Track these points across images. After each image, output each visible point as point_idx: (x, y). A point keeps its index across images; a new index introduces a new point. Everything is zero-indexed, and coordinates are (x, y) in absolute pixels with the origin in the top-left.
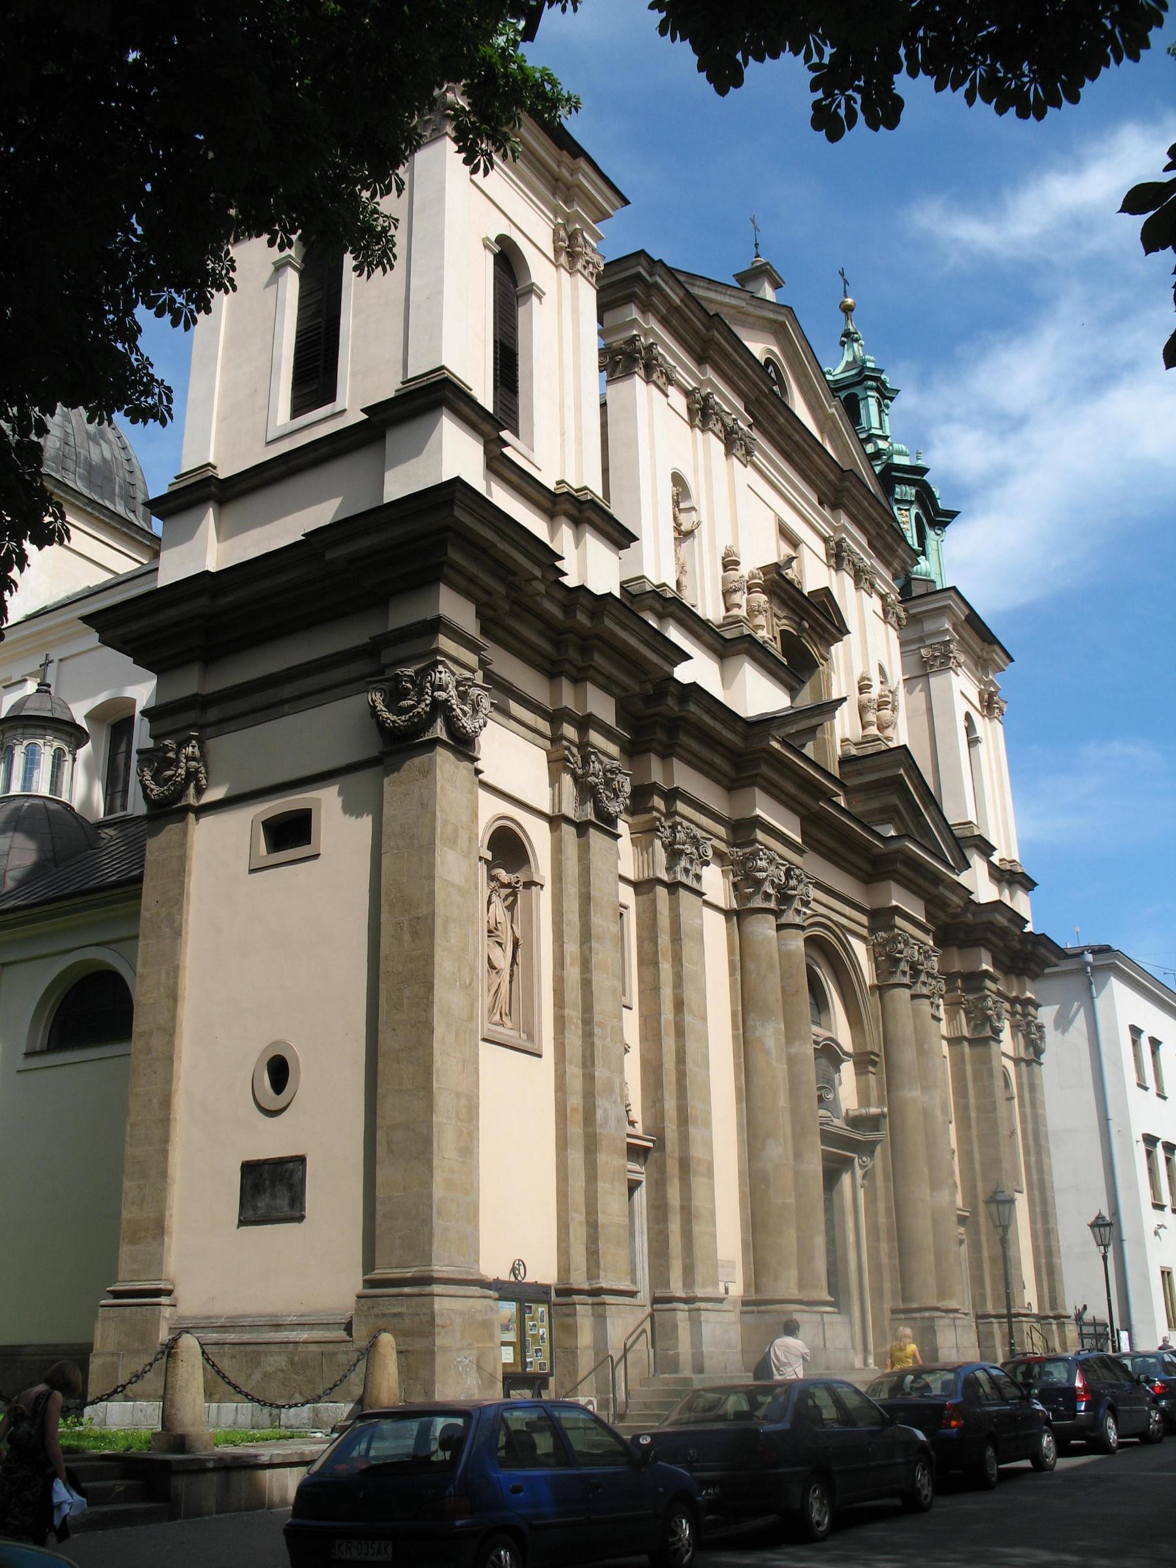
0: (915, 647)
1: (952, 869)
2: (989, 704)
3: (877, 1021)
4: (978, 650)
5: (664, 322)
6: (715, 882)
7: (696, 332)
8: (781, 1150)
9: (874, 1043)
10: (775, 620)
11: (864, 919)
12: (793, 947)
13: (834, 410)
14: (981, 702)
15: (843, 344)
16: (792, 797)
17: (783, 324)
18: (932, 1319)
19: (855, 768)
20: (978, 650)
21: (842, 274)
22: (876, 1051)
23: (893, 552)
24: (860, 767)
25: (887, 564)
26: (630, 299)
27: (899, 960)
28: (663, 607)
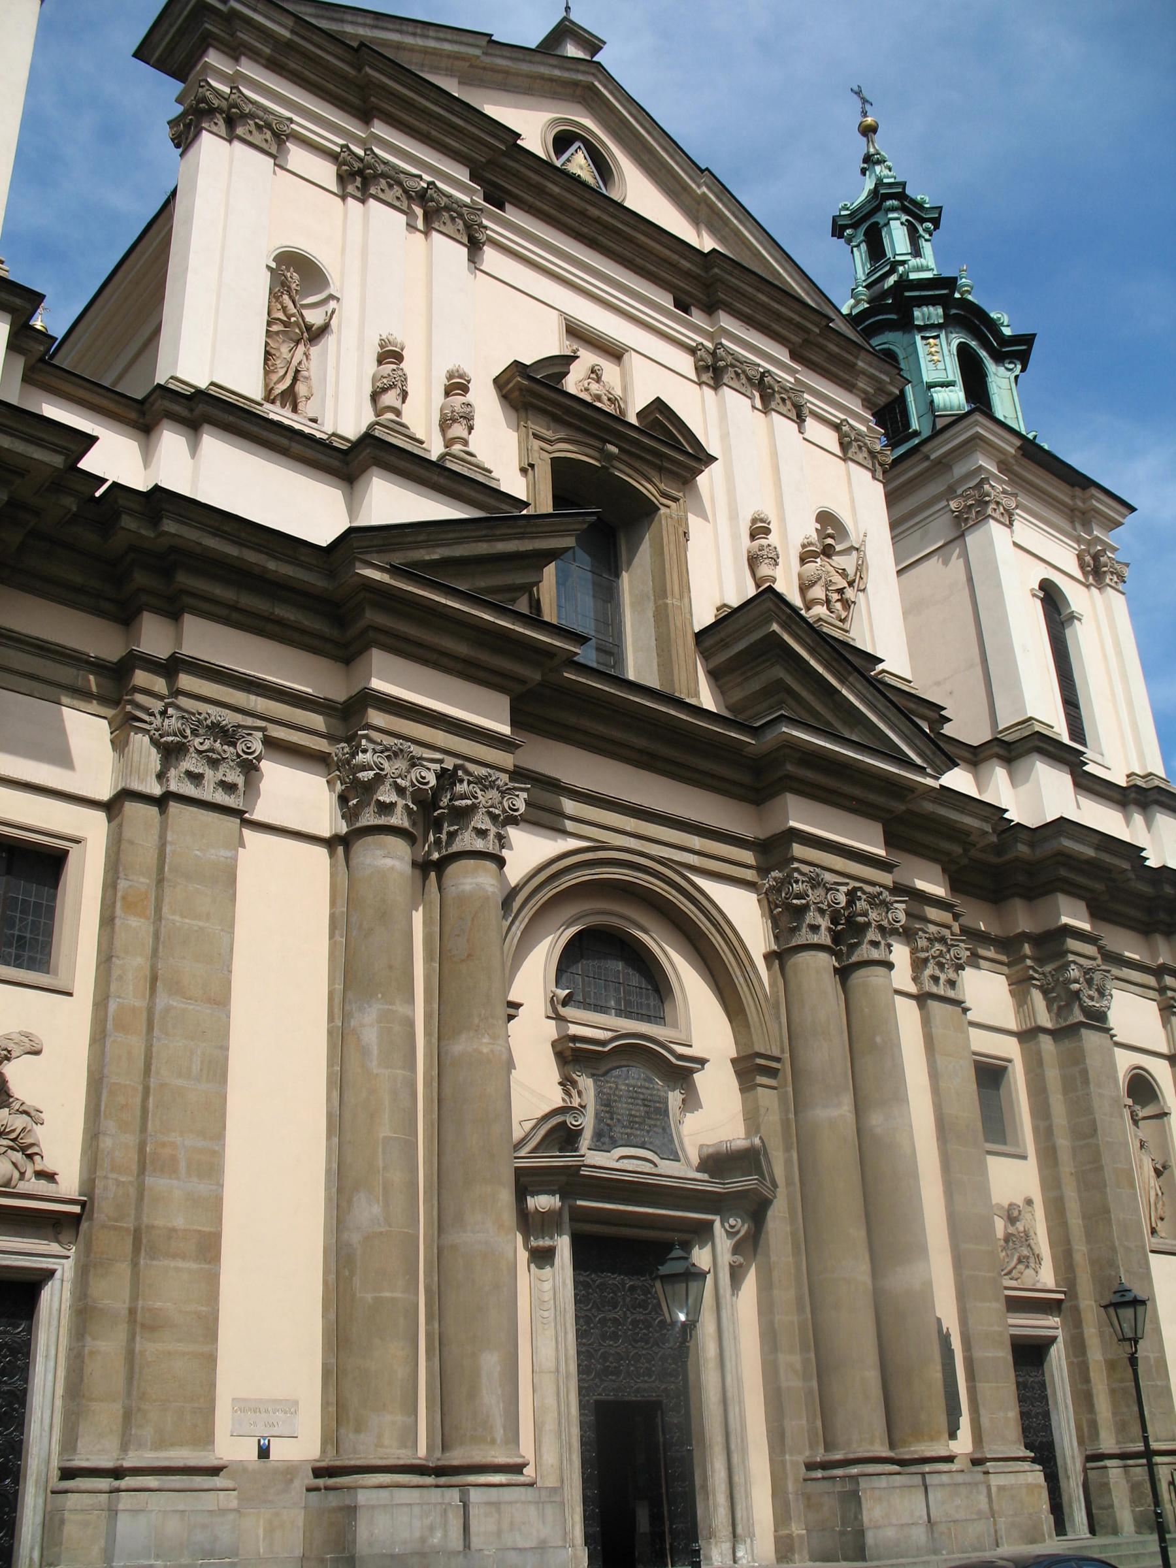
0: (944, 503)
1: (921, 770)
2: (1096, 570)
3: (776, 1006)
4: (1067, 500)
5: (274, 65)
6: (297, 794)
8: (376, 1209)
9: (769, 1041)
10: (537, 444)
11: (748, 857)
12: (468, 888)
13: (705, 189)
14: (1082, 565)
15: (863, 172)
17: (591, 88)
18: (854, 1478)
19: (717, 638)
20: (1067, 500)
21: (858, 93)
22: (776, 1052)
23: (850, 367)
24: (723, 634)
25: (849, 387)
26: (205, 42)
27: (806, 907)
28: (191, 410)
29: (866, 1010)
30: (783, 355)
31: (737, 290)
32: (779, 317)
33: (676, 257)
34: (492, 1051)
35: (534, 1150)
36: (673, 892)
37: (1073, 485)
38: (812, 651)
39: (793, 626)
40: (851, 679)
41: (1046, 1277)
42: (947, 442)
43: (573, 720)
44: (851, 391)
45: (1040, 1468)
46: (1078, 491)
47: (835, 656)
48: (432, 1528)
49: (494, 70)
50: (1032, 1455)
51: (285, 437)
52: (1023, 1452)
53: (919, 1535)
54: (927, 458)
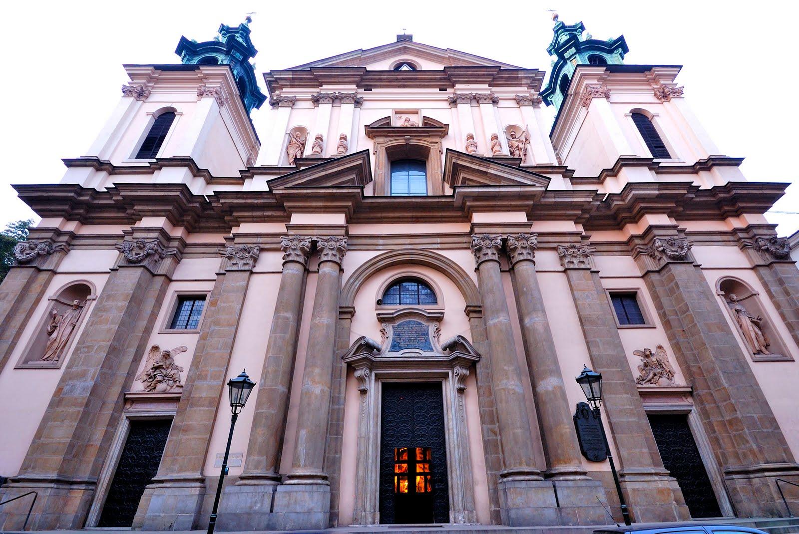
5: (292, 86)
7: (310, 79)
16: (325, 207)
17: (405, 48)
25: (520, 85)
29: (520, 280)
30: (486, 86)
31: (459, 75)
32: (478, 76)
33: (434, 77)
34: (319, 322)
35: (353, 354)
36: (429, 258)
37: (643, 72)
38: (472, 163)
39: (461, 158)
40: (491, 166)
41: (680, 381)
42: (573, 86)
43: (379, 215)
45: (675, 479)
46: (647, 73)
47: (481, 160)
48: (256, 503)
49: (369, 58)
50: (669, 472)
51: (277, 170)
52: (662, 469)
53: (551, 514)
54: (571, 95)
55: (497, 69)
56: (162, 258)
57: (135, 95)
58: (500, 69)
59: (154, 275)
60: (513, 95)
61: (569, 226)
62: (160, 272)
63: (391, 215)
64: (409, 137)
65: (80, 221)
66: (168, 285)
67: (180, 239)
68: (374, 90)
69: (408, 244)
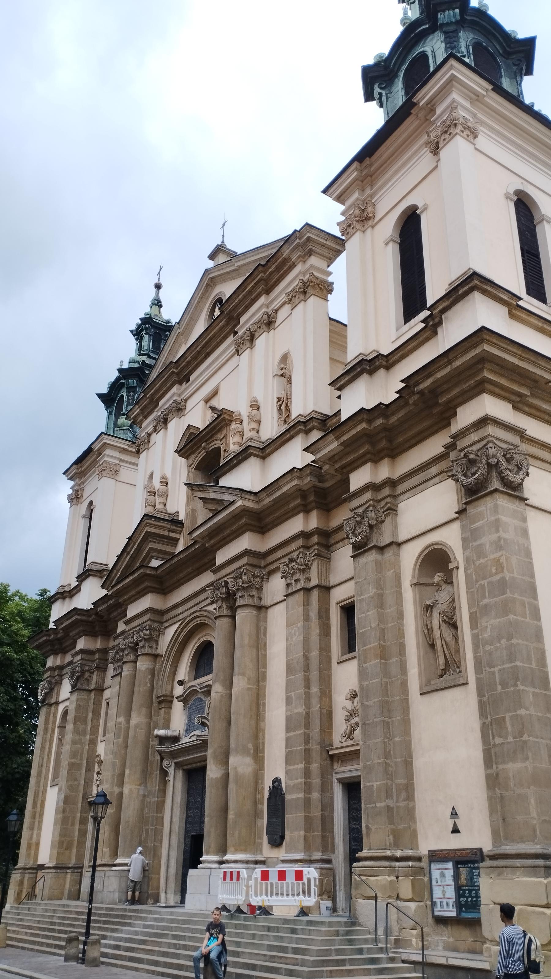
23: (285, 260)
25: (293, 266)
31: (236, 307)
32: (250, 292)
44: (296, 266)
55: (260, 269)
56: (93, 673)
57: (74, 501)
58: (263, 266)
59: (90, 691)
60: (283, 298)
61: (296, 525)
62: (93, 686)
63: (181, 575)
64: (203, 445)
65: (61, 653)
66: (102, 695)
67: (98, 650)
68: (192, 377)
69: (194, 606)
